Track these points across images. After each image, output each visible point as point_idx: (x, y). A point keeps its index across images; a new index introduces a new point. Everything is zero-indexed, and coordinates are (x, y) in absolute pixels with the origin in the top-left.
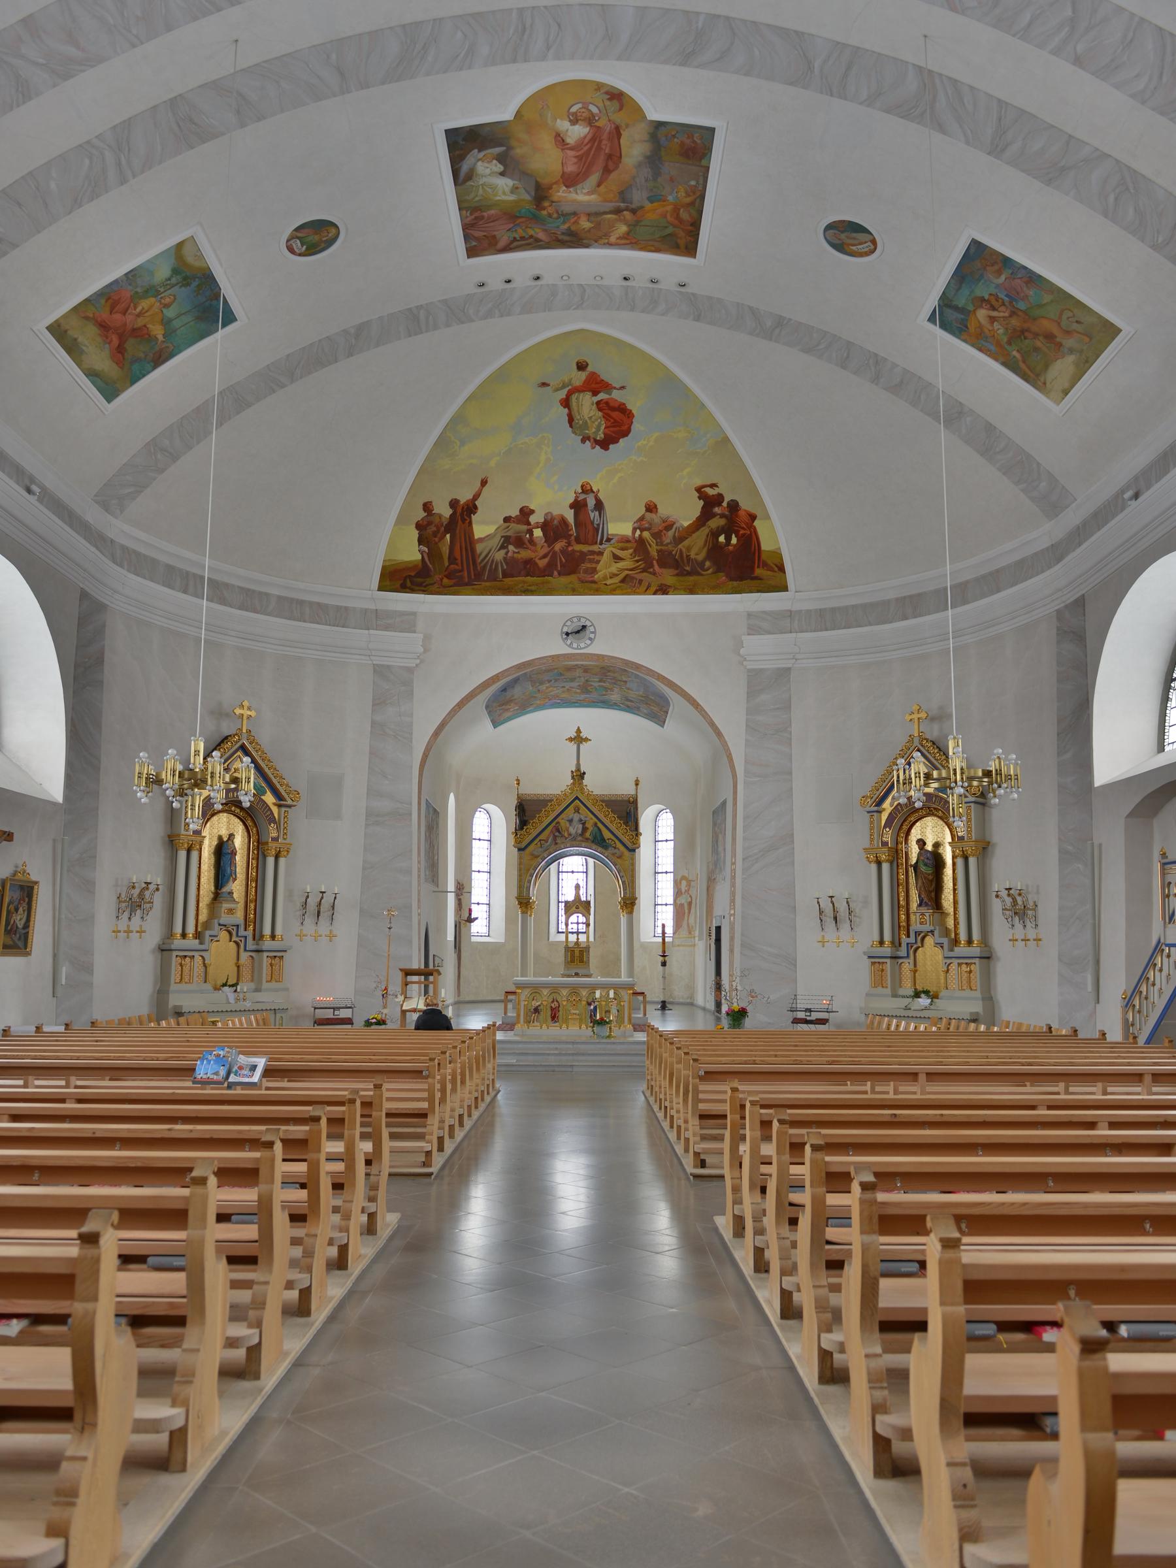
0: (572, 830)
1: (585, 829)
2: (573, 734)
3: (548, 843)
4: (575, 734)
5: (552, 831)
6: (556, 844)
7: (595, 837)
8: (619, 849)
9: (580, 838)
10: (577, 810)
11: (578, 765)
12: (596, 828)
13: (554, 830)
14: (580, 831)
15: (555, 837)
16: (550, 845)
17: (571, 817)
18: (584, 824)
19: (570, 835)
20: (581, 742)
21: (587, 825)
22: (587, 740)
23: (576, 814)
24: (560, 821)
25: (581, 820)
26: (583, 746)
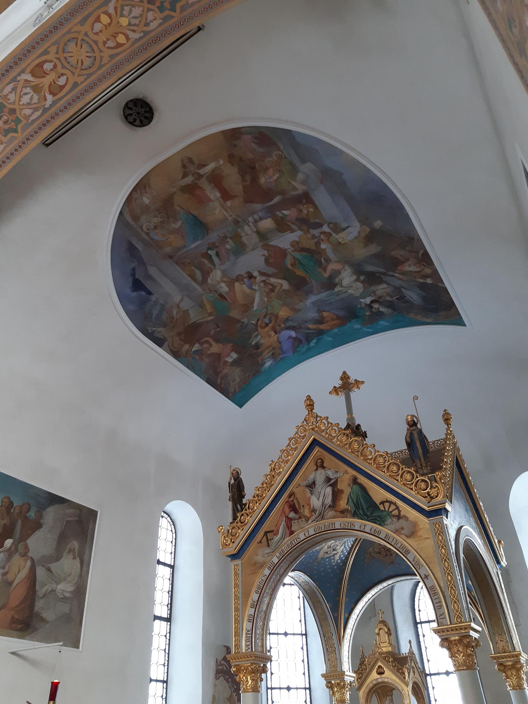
0: (316, 502)
1: (336, 494)
2: (338, 383)
3: (279, 536)
4: (340, 382)
5: (283, 512)
6: (292, 533)
7: (357, 505)
8: (406, 518)
9: (331, 513)
10: (320, 465)
11: (351, 418)
12: (355, 487)
13: (287, 509)
14: (329, 501)
15: (289, 520)
16: (283, 538)
17: (311, 477)
18: (334, 485)
19: (314, 511)
20: (350, 390)
21: (340, 486)
22: (358, 383)
23: (321, 471)
24: (295, 490)
25: (328, 479)
26: (355, 394)
